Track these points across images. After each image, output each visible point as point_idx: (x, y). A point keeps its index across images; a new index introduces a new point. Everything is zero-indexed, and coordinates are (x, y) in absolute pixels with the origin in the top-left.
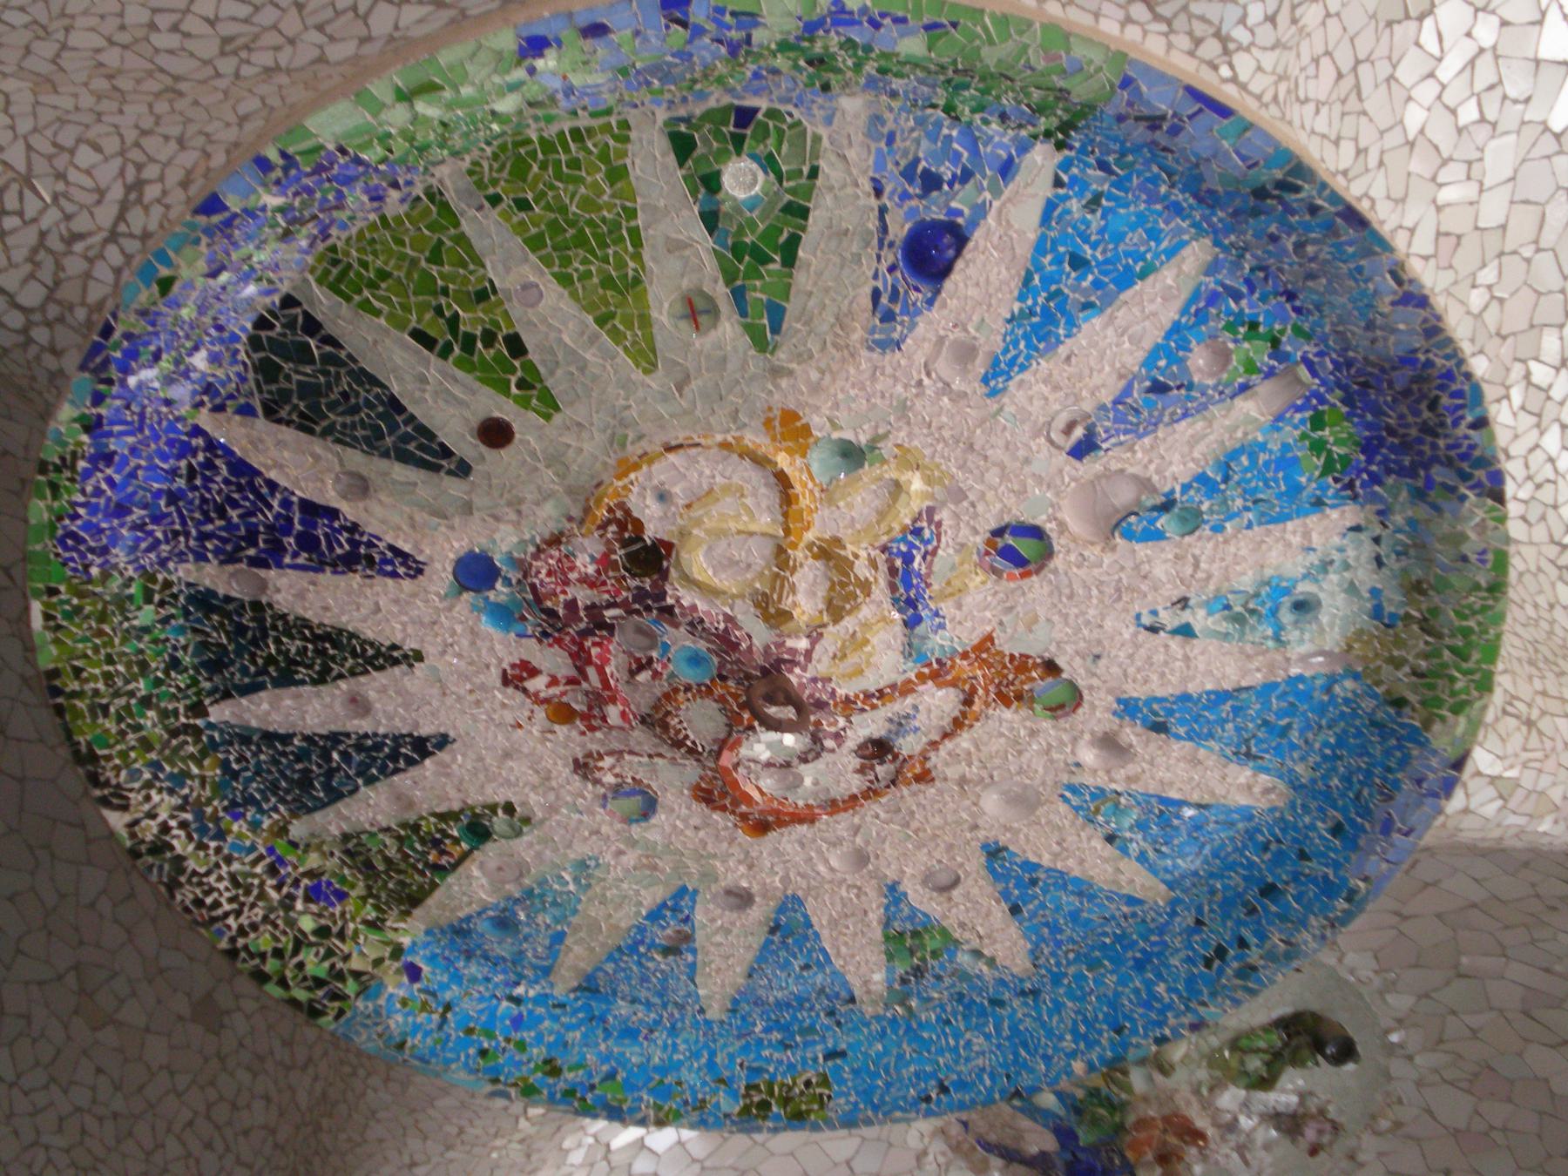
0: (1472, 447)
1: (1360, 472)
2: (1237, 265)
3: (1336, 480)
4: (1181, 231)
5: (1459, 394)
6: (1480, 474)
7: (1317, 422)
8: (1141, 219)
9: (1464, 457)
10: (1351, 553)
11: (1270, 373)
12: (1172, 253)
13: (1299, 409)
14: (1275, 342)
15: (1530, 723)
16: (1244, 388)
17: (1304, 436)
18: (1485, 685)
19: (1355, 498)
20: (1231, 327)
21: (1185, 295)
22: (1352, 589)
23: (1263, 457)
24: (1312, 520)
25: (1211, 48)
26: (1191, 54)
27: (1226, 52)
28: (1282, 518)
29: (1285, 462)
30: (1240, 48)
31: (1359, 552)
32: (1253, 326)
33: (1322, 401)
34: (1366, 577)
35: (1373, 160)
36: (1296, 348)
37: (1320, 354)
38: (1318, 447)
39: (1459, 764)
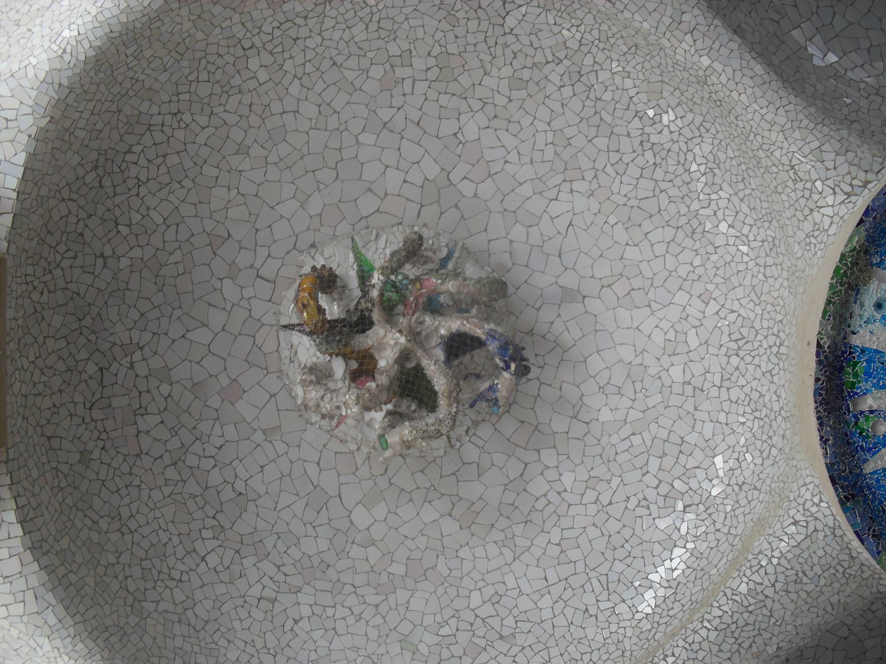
0: (821, 370)
1: (846, 358)
2: (859, 459)
3: (854, 358)
4: (870, 479)
5: (820, 395)
6: (822, 358)
7: (853, 384)
8: (879, 487)
9: (824, 367)
10: (858, 323)
11: (862, 412)
12: (875, 472)
13: (857, 394)
14: (856, 424)
15: (792, 167)
16: (871, 412)
17: (859, 382)
18: (843, 256)
19: (850, 347)
20: (868, 437)
21: (877, 456)
22: (862, 305)
23: (875, 381)
24: (867, 345)
25: (838, 532)
26: (845, 534)
27: (834, 529)
28: (877, 351)
29: (868, 374)
30: (830, 528)
31: (856, 322)
32: (860, 434)
33: (849, 393)
34: (856, 309)
35: (724, 350)
36: (850, 417)
37: (845, 414)
38: (856, 375)
39: (861, 222)
